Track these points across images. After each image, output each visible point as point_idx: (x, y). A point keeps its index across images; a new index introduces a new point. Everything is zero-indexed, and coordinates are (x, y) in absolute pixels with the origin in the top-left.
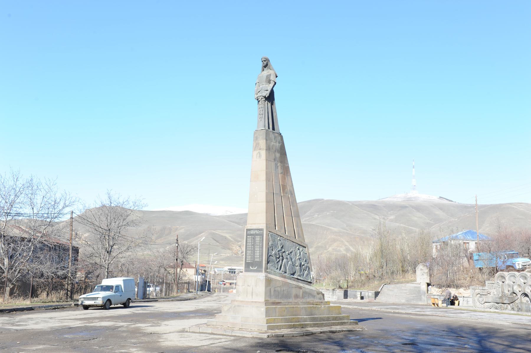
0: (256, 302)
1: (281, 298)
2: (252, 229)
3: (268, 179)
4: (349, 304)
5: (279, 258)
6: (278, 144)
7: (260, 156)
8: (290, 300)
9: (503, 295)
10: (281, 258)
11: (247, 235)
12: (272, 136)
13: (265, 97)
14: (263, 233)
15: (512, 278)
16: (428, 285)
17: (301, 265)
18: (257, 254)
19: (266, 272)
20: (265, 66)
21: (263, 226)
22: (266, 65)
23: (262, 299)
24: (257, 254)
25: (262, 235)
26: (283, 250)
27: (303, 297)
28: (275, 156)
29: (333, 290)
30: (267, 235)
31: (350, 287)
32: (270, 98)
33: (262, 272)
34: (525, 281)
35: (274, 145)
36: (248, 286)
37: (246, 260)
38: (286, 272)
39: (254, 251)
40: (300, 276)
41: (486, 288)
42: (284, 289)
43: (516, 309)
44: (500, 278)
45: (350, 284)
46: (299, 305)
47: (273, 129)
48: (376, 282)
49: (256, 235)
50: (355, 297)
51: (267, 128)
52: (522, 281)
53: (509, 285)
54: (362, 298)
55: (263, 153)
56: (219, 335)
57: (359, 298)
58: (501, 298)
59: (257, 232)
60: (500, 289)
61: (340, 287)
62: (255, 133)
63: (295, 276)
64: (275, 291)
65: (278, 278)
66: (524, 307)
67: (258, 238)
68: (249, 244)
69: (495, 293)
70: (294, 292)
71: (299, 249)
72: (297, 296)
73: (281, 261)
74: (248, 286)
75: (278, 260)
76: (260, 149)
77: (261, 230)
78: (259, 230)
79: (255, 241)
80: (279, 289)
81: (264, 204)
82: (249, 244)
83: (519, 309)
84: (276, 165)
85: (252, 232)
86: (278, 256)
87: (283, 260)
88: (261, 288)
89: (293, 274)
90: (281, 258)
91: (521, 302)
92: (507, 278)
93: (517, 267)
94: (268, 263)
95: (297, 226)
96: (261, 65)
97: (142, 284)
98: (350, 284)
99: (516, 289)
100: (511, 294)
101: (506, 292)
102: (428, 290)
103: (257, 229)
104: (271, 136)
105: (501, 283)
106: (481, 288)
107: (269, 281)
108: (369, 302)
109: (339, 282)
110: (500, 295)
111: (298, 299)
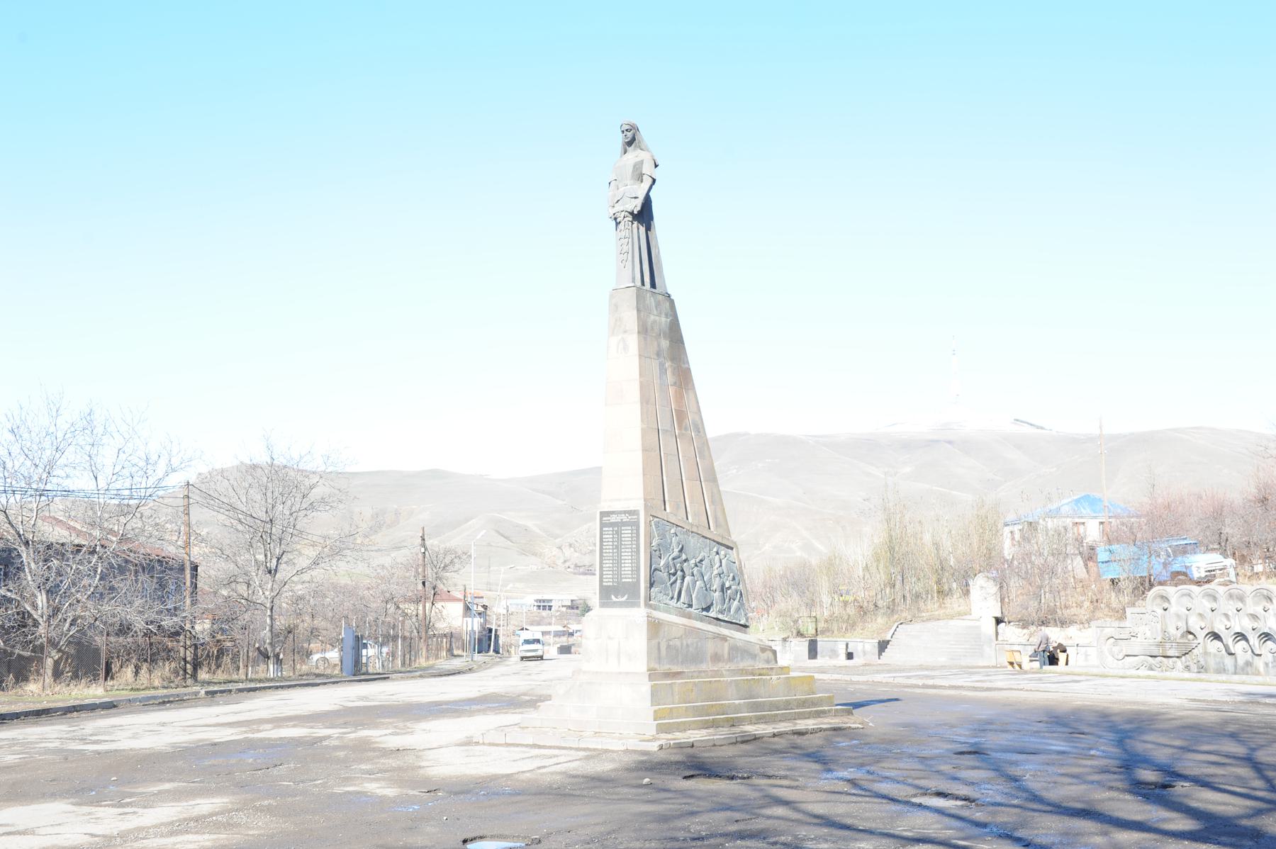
0: (627, 673)
1: (682, 663)
2: (613, 513)
3: (645, 400)
4: (822, 670)
5: (674, 574)
6: (663, 319)
7: (625, 348)
8: (704, 667)
9: (1166, 640)
10: (679, 573)
11: (602, 525)
12: (650, 301)
13: (632, 213)
15: (1185, 599)
16: (999, 621)
17: (723, 589)
18: (627, 567)
19: (647, 605)
20: (630, 143)
21: (638, 505)
22: (631, 140)
23: (641, 666)
24: (627, 567)
25: (637, 524)
26: (684, 557)
27: (730, 659)
29: (785, 640)
30: (648, 524)
31: (823, 632)
32: (644, 215)
33: (637, 605)
34: (1214, 605)
35: (655, 322)
36: (609, 638)
37: (601, 581)
38: (690, 606)
39: (618, 562)
40: (721, 612)
41: (1127, 623)
42: (689, 641)
43: (1194, 668)
44: (1159, 601)
45: (821, 625)
46: (722, 676)
47: (653, 285)
48: (880, 620)
49: (623, 524)
50: (834, 653)
51: (639, 284)
52: (1208, 604)
53: (1178, 616)
54: (850, 656)
55: (633, 341)
57: (843, 656)
58: (1160, 644)
59: (625, 518)
60: (1159, 626)
61: (800, 634)
62: (611, 296)
63: (712, 614)
64: (668, 647)
66: (1212, 663)
67: (627, 532)
68: (608, 547)
69: (1148, 634)
70: (710, 647)
72: (716, 658)
74: (609, 638)
75: (673, 579)
78: (631, 513)
79: (620, 540)
80: (678, 643)
81: (640, 454)
82: (608, 547)
83: (1202, 669)
84: (662, 365)
85: (613, 519)
86: (672, 571)
87: (683, 577)
88: (639, 642)
89: (707, 609)
90: (679, 573)
91: (1206, 653)
92: (1173, 600)
93: (1196, 575)
94: (651, 585)
95: (713, 502)
96: (620, 139)
97: (350, 642)
98: (821, 625)
99: (1195, 624)
100: (1182, 636)
101: (1172, 631)
102: (997, 633)
103: (625, 512)
104: (648, 302)
105: (1160, 611)
106: (1116, 624)
107: (655, 627)
108: (865, 665)
109: (796, 622)
110: (1159, 639)
111: (721, 665)
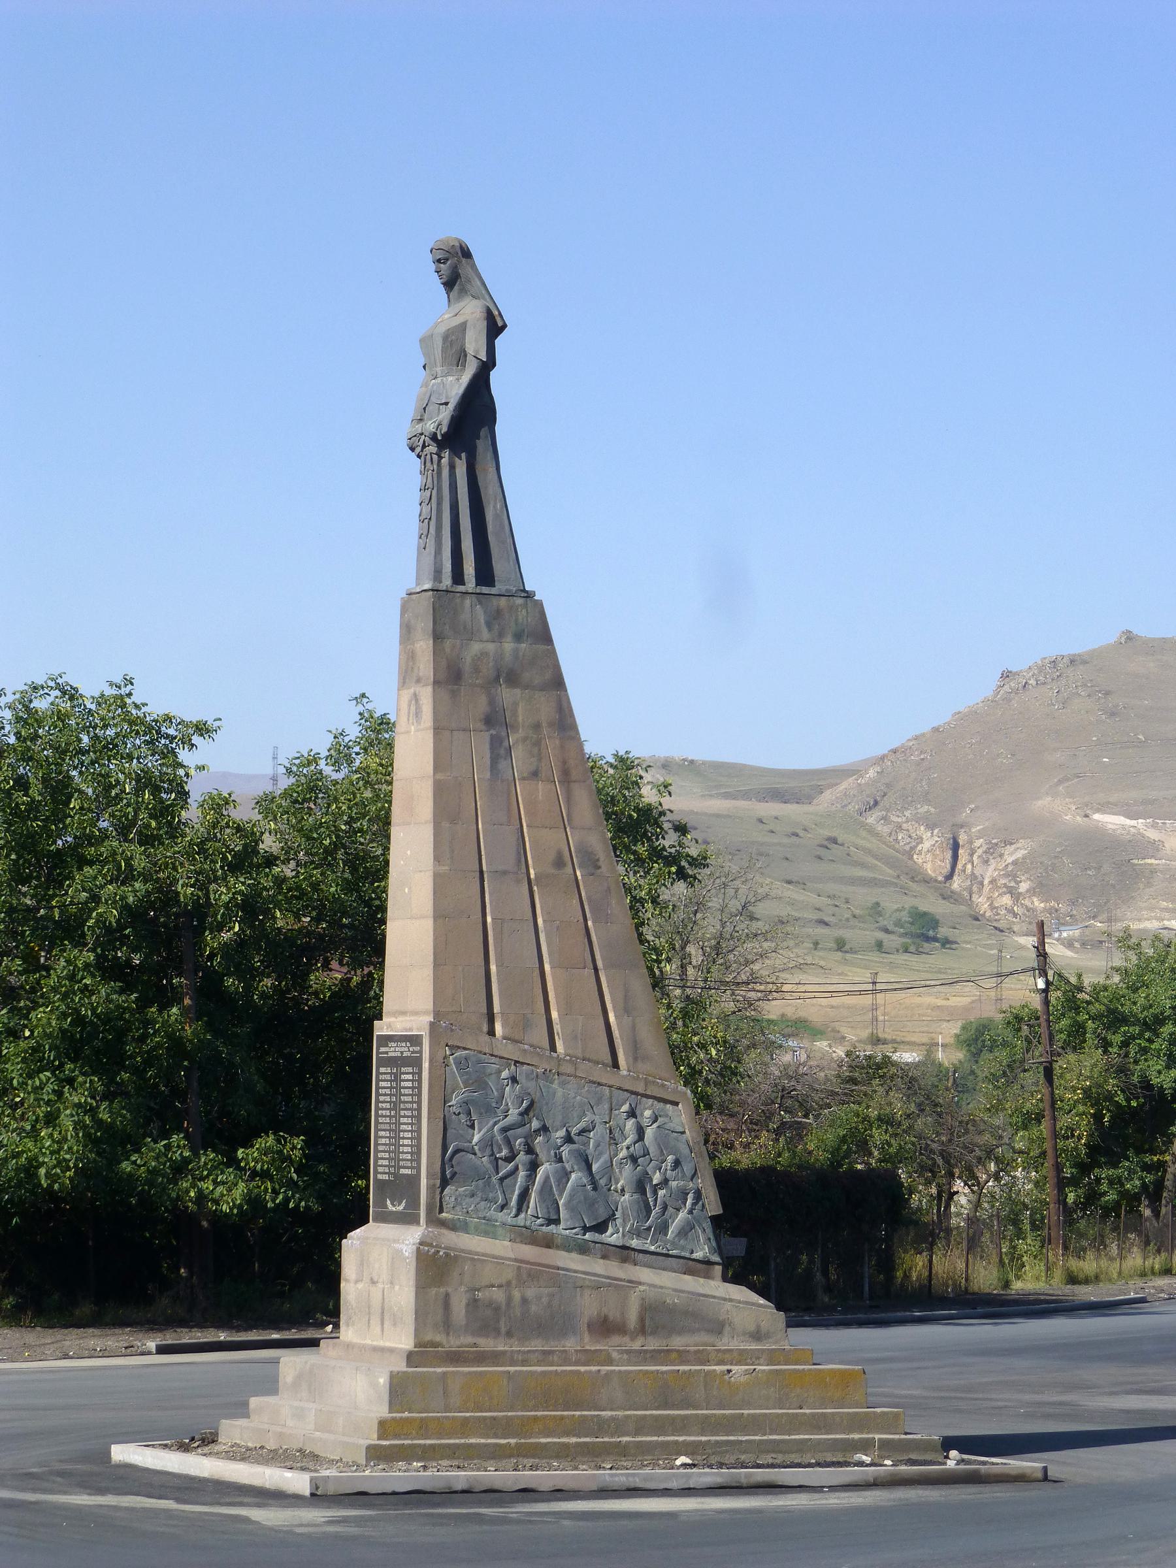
1: (509, 1334)
5: (509, 1159)
8: (570, 1344)
10: (522, 1158)
12: (472, 613)
13: (434, 437)
14: (421, 1052)
17: (641, 1186)
22: (456, 268)
25: (416, 1062)
27: (642, 1330)
28: (492, 702)
30: (441, 1064)
32: (468, 428)
33: (418, 1223)
35: (484, 654)
40: (638, 1233)
42: (530, 1293)
46: (609, 1361)
47: (485, 575)
51: (447, 581)
55: (426, 694)
56: (666, 1492)
62: (404, 609)
63: (612, 1237)
64: (473, 1304)
65: (502, 1247)
70: (588, 1306)
71: (632, 1114)
72: (605, 1327)
73: (522, 1174)
74: (373, 1282)
75: (506, 1168)
76: (418, 681)
77: (415, 1040)
80: (498, 1295)
81: (429, 924)
86: (504, 1152)
87: (534, 1166)
89: (601, 1228)
90: (522, 1158)
94: (445, 1183)
104: (465, 616)
